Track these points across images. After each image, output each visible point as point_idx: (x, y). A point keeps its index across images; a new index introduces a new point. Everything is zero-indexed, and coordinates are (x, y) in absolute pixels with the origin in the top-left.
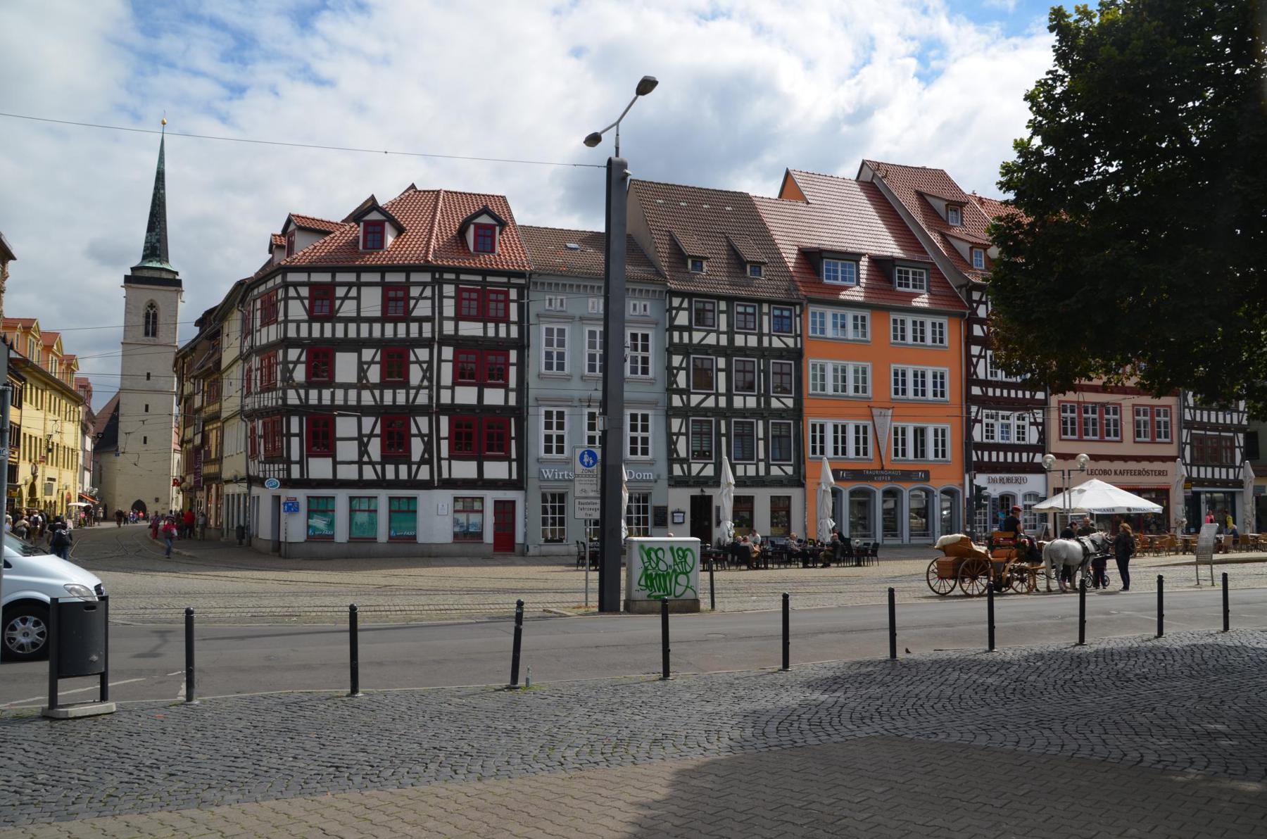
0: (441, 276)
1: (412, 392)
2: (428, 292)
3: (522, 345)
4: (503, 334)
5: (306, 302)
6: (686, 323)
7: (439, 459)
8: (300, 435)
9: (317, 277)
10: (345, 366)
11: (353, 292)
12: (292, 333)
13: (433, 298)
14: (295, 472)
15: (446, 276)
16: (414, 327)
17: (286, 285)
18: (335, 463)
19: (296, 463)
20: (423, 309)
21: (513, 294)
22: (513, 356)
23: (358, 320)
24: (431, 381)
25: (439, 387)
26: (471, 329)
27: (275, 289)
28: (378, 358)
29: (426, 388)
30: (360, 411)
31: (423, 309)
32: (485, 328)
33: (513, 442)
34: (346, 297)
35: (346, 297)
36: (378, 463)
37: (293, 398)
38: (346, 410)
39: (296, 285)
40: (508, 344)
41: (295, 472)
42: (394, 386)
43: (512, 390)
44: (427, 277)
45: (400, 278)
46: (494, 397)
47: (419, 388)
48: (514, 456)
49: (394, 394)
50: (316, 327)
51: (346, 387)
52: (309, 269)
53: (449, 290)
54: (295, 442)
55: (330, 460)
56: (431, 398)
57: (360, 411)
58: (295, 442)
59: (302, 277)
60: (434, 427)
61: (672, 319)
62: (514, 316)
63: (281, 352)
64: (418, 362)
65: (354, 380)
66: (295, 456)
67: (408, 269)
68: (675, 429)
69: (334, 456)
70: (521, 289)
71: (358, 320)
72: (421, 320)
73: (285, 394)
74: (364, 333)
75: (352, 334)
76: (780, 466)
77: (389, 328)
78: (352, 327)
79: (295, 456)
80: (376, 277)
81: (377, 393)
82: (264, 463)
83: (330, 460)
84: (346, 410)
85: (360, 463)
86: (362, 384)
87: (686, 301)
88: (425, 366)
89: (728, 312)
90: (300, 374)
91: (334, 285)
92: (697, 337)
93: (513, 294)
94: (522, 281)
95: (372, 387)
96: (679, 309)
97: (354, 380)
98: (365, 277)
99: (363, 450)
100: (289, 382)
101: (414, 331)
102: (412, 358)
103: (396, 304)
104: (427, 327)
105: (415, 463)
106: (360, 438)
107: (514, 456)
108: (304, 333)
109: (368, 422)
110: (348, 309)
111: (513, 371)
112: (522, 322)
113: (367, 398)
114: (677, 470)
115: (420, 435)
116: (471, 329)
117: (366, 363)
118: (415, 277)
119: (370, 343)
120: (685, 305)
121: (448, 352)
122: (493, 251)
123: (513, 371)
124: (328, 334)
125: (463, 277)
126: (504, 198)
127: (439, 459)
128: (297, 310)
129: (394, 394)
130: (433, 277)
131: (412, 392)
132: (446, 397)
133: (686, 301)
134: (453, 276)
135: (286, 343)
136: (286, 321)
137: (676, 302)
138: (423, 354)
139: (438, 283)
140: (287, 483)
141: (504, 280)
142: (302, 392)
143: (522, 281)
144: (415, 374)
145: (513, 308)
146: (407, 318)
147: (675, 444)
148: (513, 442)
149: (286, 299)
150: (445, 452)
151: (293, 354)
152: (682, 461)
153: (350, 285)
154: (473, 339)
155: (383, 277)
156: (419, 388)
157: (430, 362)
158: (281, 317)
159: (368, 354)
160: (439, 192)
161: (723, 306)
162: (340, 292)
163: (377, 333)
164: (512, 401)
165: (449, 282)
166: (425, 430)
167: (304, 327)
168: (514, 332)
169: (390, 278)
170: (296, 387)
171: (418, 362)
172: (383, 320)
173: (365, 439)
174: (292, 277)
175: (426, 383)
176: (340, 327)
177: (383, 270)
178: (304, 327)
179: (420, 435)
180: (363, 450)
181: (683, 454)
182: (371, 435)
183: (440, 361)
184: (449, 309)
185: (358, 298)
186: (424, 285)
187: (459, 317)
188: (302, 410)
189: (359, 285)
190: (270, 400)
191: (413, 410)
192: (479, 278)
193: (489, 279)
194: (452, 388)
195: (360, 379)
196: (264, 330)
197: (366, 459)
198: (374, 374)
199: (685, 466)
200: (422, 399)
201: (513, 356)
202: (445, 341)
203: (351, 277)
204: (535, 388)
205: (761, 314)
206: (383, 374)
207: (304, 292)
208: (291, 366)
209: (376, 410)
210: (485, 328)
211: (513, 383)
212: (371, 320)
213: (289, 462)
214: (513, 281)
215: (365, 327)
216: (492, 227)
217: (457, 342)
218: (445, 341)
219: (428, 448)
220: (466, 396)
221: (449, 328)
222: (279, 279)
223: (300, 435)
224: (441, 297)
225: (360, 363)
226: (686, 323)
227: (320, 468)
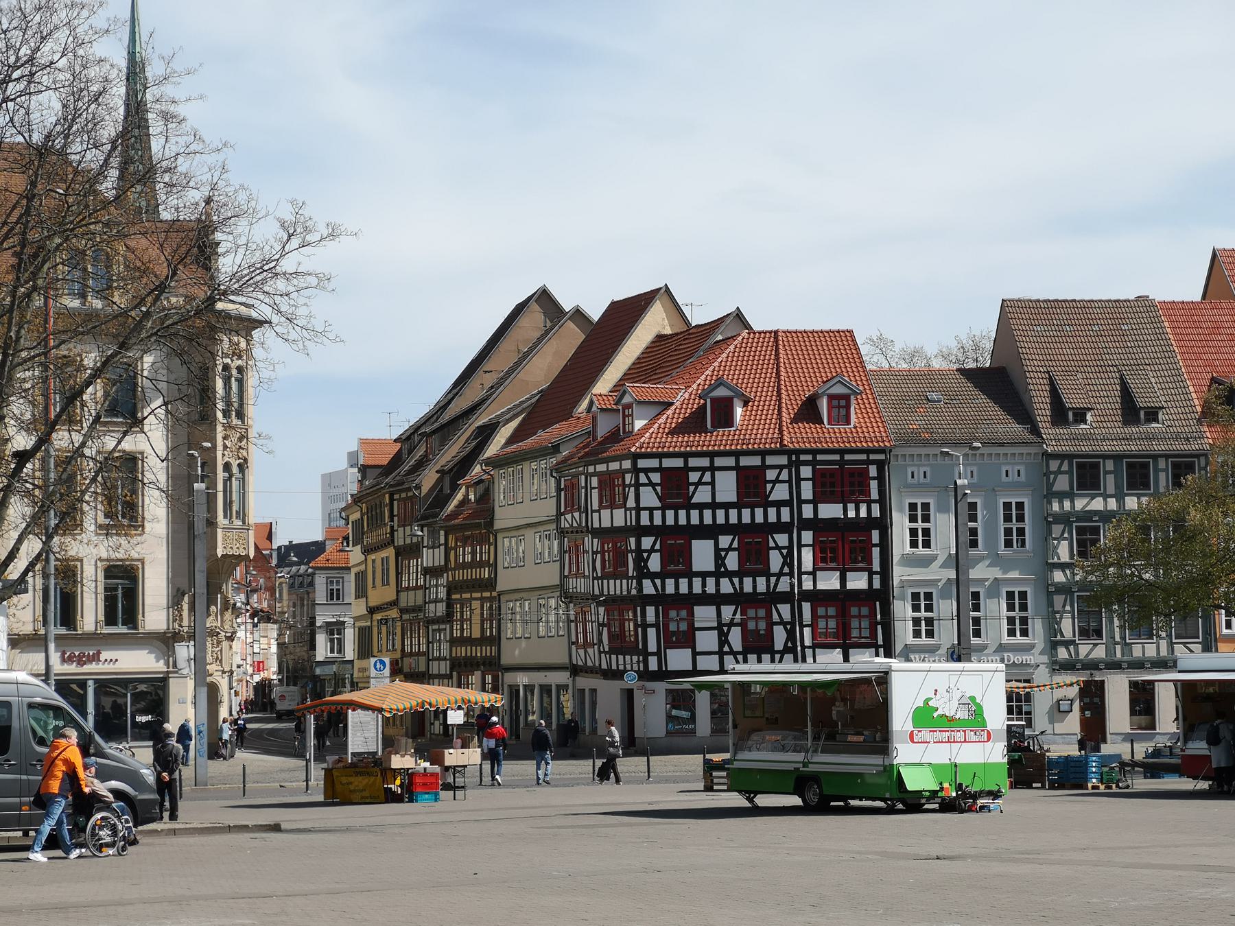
0: (798, 458)
1: (773, 579)
2: (785, 475)
3: (883, 525)
4: (863, 514)
5: (658, 488)
6: (1067, 488)
7: (803, 647)
8: (656, 625)
9: (668, 463)
10: (702, 554)
11: (707, 477)
12: (645, 521)
13: (790, 481)
14: (653, 664)
15: (803, 457)
16: (772, 512)
17: (636, 471)
18: (695, 654)
19: (653, 654)
20: (780, 493)
21: (873, 471)
22: (875, 536)
23: (714, 506)
24: (791, 566)
25: (800, 573)
26: (830, 511)
27: (622, 473)
28: (735, 545)
29: (786, 574)
30: (718, 600)
31: (780, 493)
32: (845, 511)
33: (879, 627)
34: (700, 483)
35: (700, 483)
36: (739, 653)
37: (648, 588)
38: (704, 599)
39: (646, 471)
40: (871, 523)
41: (653, 664)
42: (754, 574)
43: (876, 573)
44: (783, 460)
45: (755, 461)
46: (858, 582)
47: (780, 575)
48: (880, 642)
49: (754, 582)
50: (670, 514)
51: (704, 575)
52: (660, 456)
53: (806, 472)
54: (651, 632)
55: (688, 652)
56: (792, 586)
57: (718, 600)
58: (651, 632)
59: (654, 463)
60: (797, 613)
61: (1050, 485)
62: (875, 495)
63: (633, 540)
64: (777, 547)
65: (711, 567)
66: (652, 647)
67: (763, 453)
68: (1058, 607)
69: (693, 648)
70: (881, 465)
71: (714, 506)
72: (779, 504)
73: (640, 584)
74: (721, 520)
75: (708, 520)
76: (1184, 644)
77: (746, 513)
78: (708, 514)
79: (652, 647)
80: (730, 461)
81: (736, 580)
82: (610, 652)
83: (688, 652)
84: (704, 599)
85: (721, 654)
86: (720, 572)
87: (1066, 462)
88: (785, 552)
89: (1117, 472)
90: (654, 563)
91: (687, 469)
92: (1080, 504)
93: (873, 471)
94: (882, 457)
95: (730, 575)
96: (1059, 472)
97: (711, 567)
98: (719, 462)
99: (723, 639)
100: (643, 572)
101: (772, 517)
102: (772, 544)
103: (752, 486)
104: (785, 511)
105: (778, 652)
106: (719, 627)
107: (880, 642)
108: (658, 521)
109: (727, 612)
110: (702, 495)
111: (876, 552)
112: (883, 501)
113: (726, 587)
114: (1062, 653)
115: (782, 623)
116: (830, 511)
117: (723, 550)
118: (770, 460)
119: (727, 529)
120: (1065, 467)
121: (807, 536)
122: (848, 423)
123: (876, 552)
124: (682, 521)
125: (819, 457)
126: (850, 332)
127: (803, 647)
128: (649, 498)
129: (754, 582)
130: (790, 459)
131: (773, 579)
132: (808, 585)
133: (1066, 462)
134: (809, 457)
135: (640, 531)
136: (638, 509)
137: (1054, 465)
138: (782, 539)
139: (794, 465)
140: (646, 675)
141: (864, 457)
142: (658, 582)
143: (882, 457)
144: (775, 561)
145: (874, 485)
146: (766, 504)
147: (1059, 623)
148: (879, 627)
149: (638, 485)
150: (808, 642)
151: (647, 542)
152: (1067, 644)
153: (703, 470)
154: (834, 521)
155: (737, 461)
156: (780, 575)
157: (790, 548)
158: (631, 503)
159: (724, 541)
160: (776, 332)
161: (1110, 465)
162: (694, 477)
163: (733, 520)
164: (877, 584)
165: (806, 463)
166: (787, 616)
167: (658, 515)
168: (876, 513)
169: (745, 461)
170: (652, 576)
171: (777, 547)
172: (738, 506)
173: (725, 629)
174: (642, 463)
175: (786, 570)
176: (695, 514)
177: (737, 454)
178: (658, 515)
179: (782, 623)
180: (723, 639)
181: (1068, 635)
182: (732, 624)
183: (800, 546)
184: (807, 491)
185: (712, 483)
186: (781, 468)
187: (815, 502)
188: (659, 600)
189: (713, 469)
190: (616, 587)
191: (773, 598)
192: (837, 457)
193: (847, 457)
194: (813, 573)
195: (717, 566)
196: (606, 513)
197: (726, 649)
198: (732, 562)
199: (1072, 648)
200: (784, 585)
201: (875, 536)
202: (805, 524)
203: (705, 462)
204: (899, 573)
205: (1156, 471)
206: (741, 562)
207: (656, 478)
208: (645, 555)
209: (738, 598)
210: (845, 511)
211: (876, 566)
212: (727, 506)
213: (646, 654)
214: (872, 457)
215: (720, 514)
216: (847, 398)
217: (815, 524)
218: (805, 524)
219: (791, 635)
220: (829, 582)
221: (808, 511)
222: (627, 464)
223: (656, 625)
224: (799, 480)
225: (717, 550)
226: (1067, 488)
227: (678, 659)
